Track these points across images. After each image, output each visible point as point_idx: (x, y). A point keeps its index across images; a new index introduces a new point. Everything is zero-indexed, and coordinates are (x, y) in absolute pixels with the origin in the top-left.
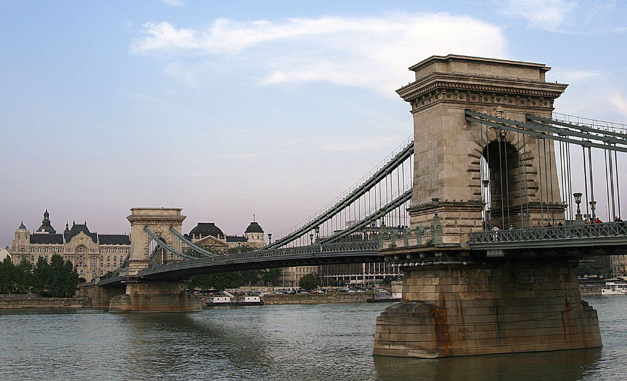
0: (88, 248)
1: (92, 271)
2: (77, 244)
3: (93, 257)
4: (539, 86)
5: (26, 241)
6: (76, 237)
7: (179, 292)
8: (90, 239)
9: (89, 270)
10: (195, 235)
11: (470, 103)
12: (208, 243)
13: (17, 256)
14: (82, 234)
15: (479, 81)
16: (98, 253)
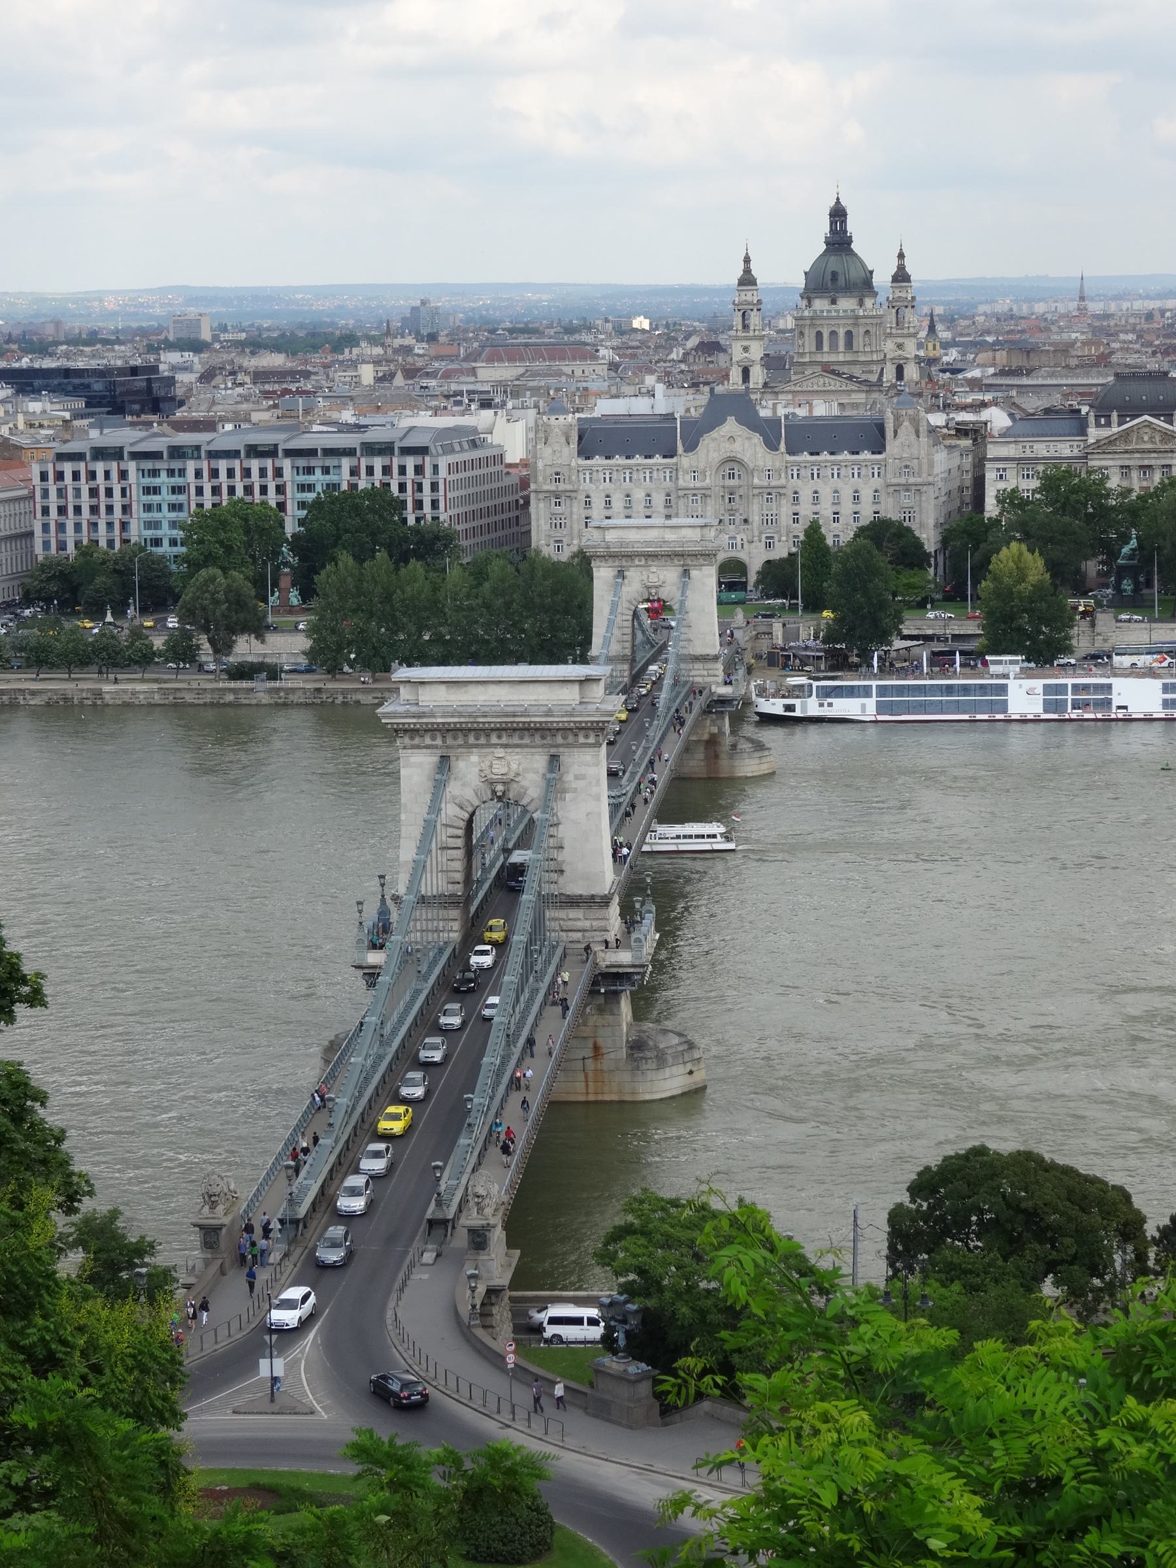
0: (751, 466)
1: (764, 536)
2: (715, 457)
3: (772, 494)
4: (563, 716)
5: (566, 451)
6: (714, 434)
7: (706, 737)
8: (757, 439)
9: (756, 533)
10: (1097, 417)
11: (447, 747)
12: (1140, 439)
13: (541, 496)
14: (731, 425)
15: (452, 716)
16: (783, 481)
